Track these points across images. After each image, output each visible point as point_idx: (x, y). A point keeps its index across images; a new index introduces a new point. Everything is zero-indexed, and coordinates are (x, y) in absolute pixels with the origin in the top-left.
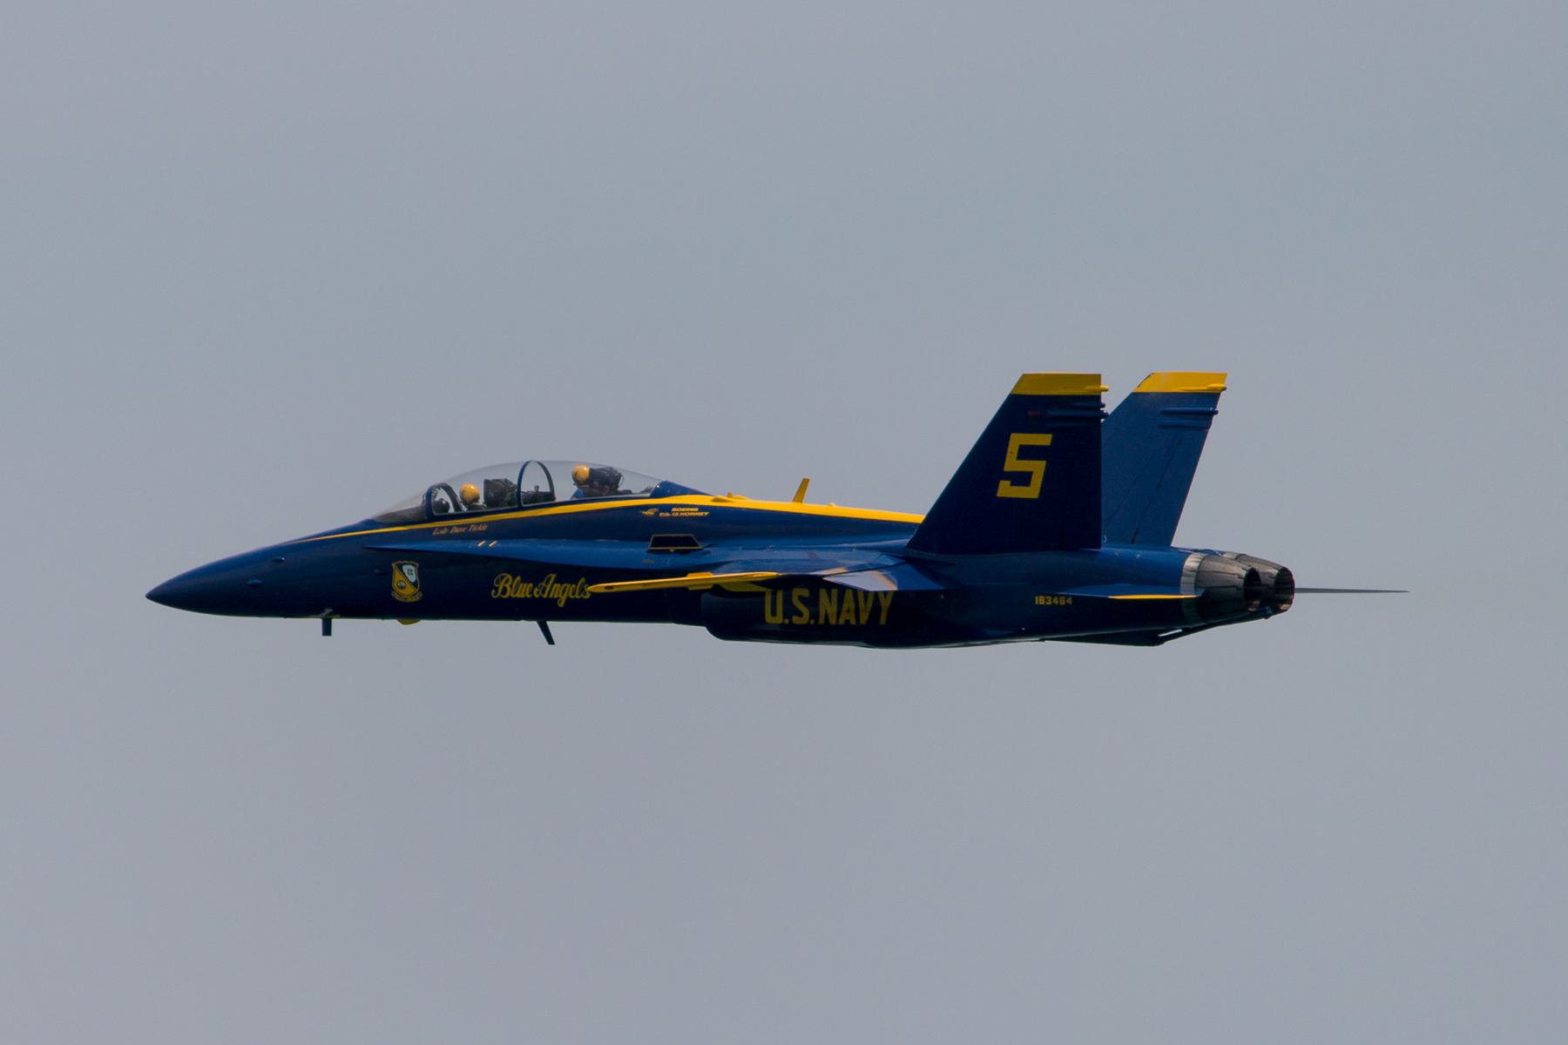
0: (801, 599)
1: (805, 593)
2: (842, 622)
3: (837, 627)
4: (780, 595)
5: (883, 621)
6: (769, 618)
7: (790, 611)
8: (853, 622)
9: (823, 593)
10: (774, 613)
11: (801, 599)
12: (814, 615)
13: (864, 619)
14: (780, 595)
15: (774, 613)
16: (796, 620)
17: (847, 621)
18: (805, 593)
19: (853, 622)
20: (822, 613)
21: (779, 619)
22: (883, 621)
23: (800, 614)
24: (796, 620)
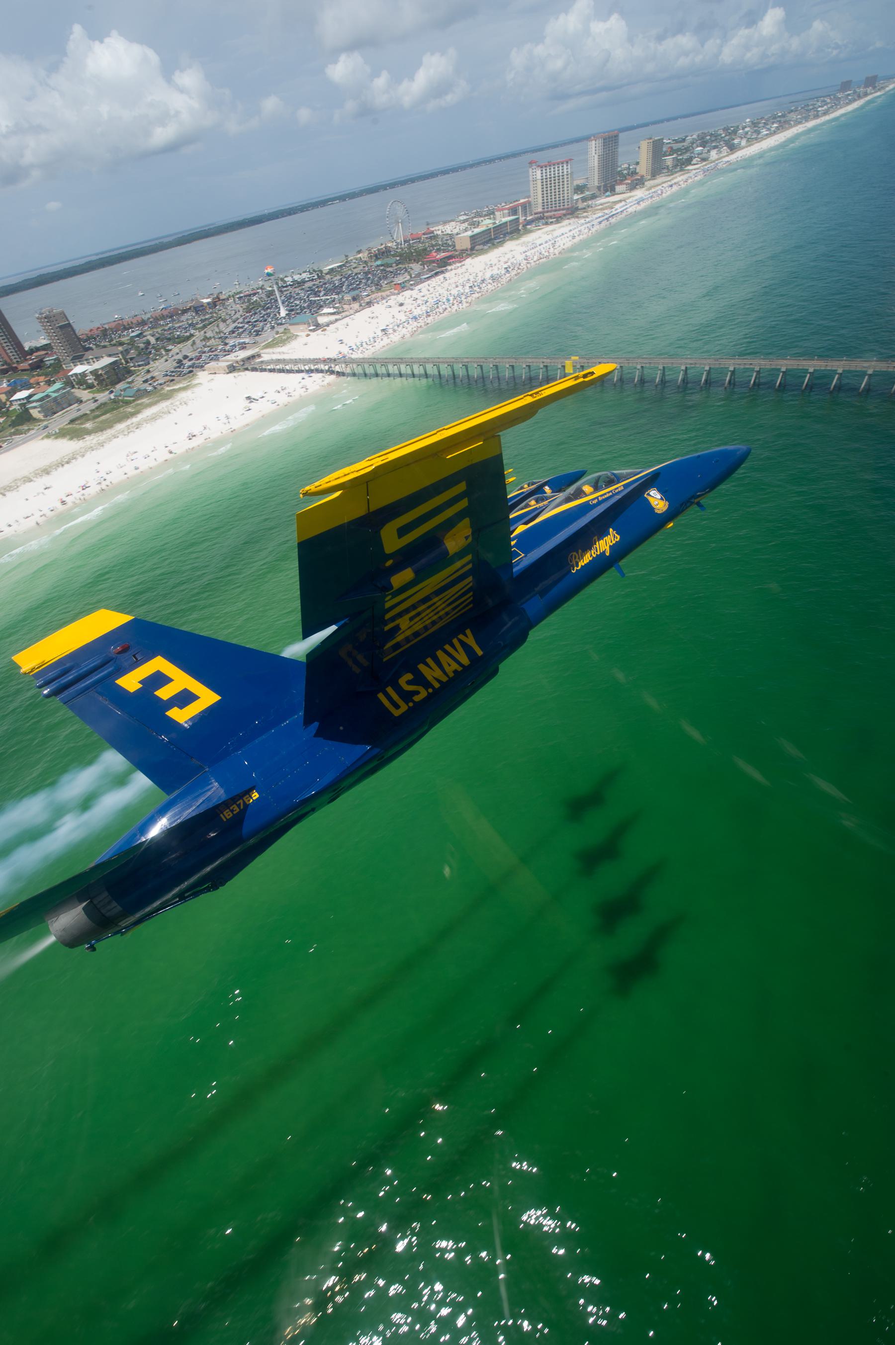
0: (409, 683)
1: (409, 676)
2: (451, 675)
3: (451, 680)
4: (389, 690)
5: (480, 653)
6: (397, 713)
7: (407, 696)
8: (460, 669)
9: (421, 667)
10: (397, 706)
11: (409, 683)
12: (426, 684)
13: (465, 661)
14: (389, 690)
15: (397, 706)
16: (417, 698)
17: (455, 672)
18: (409, 676)
19: (460, 669)
20: (430, 678)
21: (404, 708)
22: (480, 653)
23: (418, 693)
24: (417, 698)
